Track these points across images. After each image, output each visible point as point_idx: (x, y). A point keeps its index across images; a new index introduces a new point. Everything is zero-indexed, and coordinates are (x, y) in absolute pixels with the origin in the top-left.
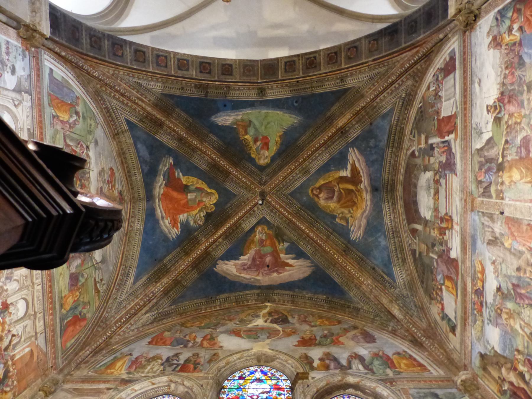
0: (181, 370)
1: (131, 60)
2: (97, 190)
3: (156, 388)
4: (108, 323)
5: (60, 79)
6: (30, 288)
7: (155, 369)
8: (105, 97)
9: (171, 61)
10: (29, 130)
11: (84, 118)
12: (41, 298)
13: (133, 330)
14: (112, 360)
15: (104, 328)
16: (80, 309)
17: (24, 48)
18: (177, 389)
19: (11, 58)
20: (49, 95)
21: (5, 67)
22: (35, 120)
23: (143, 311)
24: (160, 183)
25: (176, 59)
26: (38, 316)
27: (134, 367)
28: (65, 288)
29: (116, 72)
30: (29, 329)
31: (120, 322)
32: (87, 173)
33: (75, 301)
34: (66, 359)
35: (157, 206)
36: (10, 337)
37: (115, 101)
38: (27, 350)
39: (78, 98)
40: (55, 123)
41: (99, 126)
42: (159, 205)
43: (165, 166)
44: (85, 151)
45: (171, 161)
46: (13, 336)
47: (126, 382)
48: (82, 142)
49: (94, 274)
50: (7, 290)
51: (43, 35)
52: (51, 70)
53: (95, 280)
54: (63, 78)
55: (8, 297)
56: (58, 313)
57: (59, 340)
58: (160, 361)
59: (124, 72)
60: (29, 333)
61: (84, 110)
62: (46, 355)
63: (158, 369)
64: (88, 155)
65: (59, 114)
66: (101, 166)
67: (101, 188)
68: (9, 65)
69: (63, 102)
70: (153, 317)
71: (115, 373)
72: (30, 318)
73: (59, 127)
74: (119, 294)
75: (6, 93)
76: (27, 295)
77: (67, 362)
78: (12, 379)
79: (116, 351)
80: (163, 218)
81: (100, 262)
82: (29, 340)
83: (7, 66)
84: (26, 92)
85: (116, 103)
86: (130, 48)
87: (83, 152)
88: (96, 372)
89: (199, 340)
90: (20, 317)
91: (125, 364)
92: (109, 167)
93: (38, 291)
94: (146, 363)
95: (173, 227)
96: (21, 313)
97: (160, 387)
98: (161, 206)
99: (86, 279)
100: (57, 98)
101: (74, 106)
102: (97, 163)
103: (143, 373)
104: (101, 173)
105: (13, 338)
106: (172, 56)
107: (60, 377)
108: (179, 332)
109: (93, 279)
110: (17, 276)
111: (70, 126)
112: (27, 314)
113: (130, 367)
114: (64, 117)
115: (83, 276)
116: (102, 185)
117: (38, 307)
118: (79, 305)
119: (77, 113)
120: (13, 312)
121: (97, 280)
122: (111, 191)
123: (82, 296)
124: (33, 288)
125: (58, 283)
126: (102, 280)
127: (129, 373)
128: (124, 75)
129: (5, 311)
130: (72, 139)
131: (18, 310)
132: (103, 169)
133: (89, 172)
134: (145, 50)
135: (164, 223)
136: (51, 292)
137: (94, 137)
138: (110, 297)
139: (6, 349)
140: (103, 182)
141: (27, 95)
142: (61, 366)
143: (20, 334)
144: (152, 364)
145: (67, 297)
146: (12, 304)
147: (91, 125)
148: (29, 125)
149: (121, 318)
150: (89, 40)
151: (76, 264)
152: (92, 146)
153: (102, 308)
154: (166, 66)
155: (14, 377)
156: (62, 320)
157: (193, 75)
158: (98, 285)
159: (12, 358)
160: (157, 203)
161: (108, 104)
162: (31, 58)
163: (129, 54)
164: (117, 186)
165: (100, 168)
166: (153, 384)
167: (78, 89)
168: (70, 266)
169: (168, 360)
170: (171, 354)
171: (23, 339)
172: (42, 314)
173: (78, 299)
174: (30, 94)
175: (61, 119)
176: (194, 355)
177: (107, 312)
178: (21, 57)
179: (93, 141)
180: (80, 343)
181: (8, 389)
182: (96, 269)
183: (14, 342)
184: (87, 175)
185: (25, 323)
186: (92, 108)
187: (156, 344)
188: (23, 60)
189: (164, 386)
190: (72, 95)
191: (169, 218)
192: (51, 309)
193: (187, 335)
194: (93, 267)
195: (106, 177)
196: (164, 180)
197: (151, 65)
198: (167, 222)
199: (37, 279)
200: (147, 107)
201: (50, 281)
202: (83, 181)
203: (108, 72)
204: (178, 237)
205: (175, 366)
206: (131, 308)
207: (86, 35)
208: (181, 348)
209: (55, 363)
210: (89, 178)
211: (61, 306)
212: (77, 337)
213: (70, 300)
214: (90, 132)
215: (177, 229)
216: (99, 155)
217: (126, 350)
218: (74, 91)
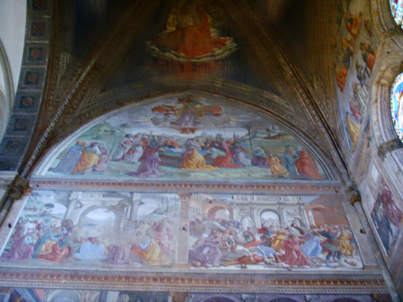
0: (371, 68)
1: (36, 88)
2: (173, 128)
3: (381, 98)
4: (314, 128)
5: (59, 161)
6: (253, 206)
7: (364, 95)
8: (77, 114)
9: (35, 44)
10: (104, 196)
11: (98, 138)
12: (265, 197)
13: (327, 104)
14: (347, 133)
15: (318, 133)
16: (290, 157)
17: (30, 194)
18: (388, 78)
19: (39, 207)
20: (73, 173)
21: (47, 213)
22: (95, 189)
23: (310, 89)
24: (173, 56)
25: (33, 38)
26: (282, 201)
27: (358, 115)
28: (264, 171)
29: (51, 103)
30: (291, 211)
31: (315, 116)
32: (154, 139)
33: (281, 163)
34: (334, 176)
35: (199, 61)
36: (293, 229)
37: (82, 104)
38: (310, 213)
39: (78, 143)
40: (100, 170)
41: (107, 121)
42: (198, 59)
43: (154, 49)
44: (131, 139)
45: (148, 43)
46: (292, 225)
47: (367, 127)
48: (122, 143)
49: (259, 139)
50: (249, 228)
51: (17, 178)
52: (50, 169)
53: (266, 138)
54: (57, 158)
55: (255, 227)
56: (286, 181)
57: (313, 182)
58: (359, 87)
59: (51, 95)
60: (295, 210)
61: (90, 137)
62: (322, 196)
63: (365, 92)
64: (136, 136)
65: (92, 165)
66: (148, 121)
67: (172, 123)
68: (45, 209)
69: (80, 160)
70: (319, 79)
71: (358, 134)
72: (282, 209)
73: (104, 166)
74: (287, 112)
75: (69, 214)
76: (259, 210)
77: (337, 176)
78: (332, 229)
79: (342, 126)
80: (213, 56)
81: (249, 130)
82: (301, 212)
83: (45, 211)
84: (70, 196)
85: (83, 102)
86: (24, 88)
87: (132, 142)
88: (353, 151)
89: (349, 37)
90: (278, 218)
91: (354, 122)
92: (151, 112)
93: (258, 199)
94: (357, 101)
95: (224, 44)
96: (274, 216)
97: (381, 95)
98: (199, 57)
99: (262, 148)
100: (77, 165)
101: (86, 148)
102: (146, 127)
103: (364, 108)
104: (156, 122)
105: (295, 225)
106: (29, 42)
107: (349, 184)
108: (338, 56)
109: (264, 140)
110: (238, 218)
111: (105, 154)
112: (277, 211)
113: (357, 119)
114: (95, 158)
115: (257, 152)
116: (168, 123)
117: (274, 200)
118: (286, 158)
119: (92, 145)
120: (270, 224)
121: (266, 136)
122: (177, 112)
123: (278, 154)
124: (254, 204)
125: (257, 179)
126: (268, 130)
127: (361, 121)
128: (53, 95)
129: (268, 231)
130: (117, 153)
131: (270, 219)
132: (152, 119)
133: (153, 136)
134: (25, 72)
135: (218, 54)
136: (263, 187)
137: (117, 128)
138: (288, 122)
139: (302, 232)
140: (166, 120)
141: (72, 195)
142: (339, 181)
143: (293, 219)
144: (359, 96)
145: (273, 170)
146: (262, 225)
147: (106, 131)
148: (100, 195)
149: (312, 114)
150: (19, 132)
151: (244, 158)
152: (127, 131)
153: (297, 133)
154: (41, 49)
155: (330, 227)
156: (293, 177)
157: (48, 19)
158: (272, 135)
159: (312, 227)
160: (196, 60)
161: (84, 111)
162: (39, 188)
163: (32, 90)
164: (173, 104)
165: (151, 124)
166: (376, 101)
167: (69, 143)
168: (244, 165)
169: (360, 78)
170: (355, 73)
171: (299, 217)
172: (282, 198)
173: (279, 159)
174: (72, 192)
175: (96, 163)
176: (361, 49)
177: (303, 128)
178: (38, 198)
179: (121, 129)
180: (324, 160)
181: (339, 234)
182: (255, 136)
183: (299, 225)
184: (156, 138)
185: (284, 213)
186: (88, 129)
187: (344, 85)
188: (41, 196)
189: (382, 90)
190: (74, 150)
191: (214, 49)
192: (280, 188)
193: (342, 48)
194: (252, 140)
195: (161, 116)
196: (170, 52)
197: (40, 67)
198: (218, 51)
199: (246, 200)
200: (87, 71)
201: (252, 187)
202: (161, 144)
203: (51, 111)
204: (235, 41)
205: (366, 74)
206: (304, 102)
207: (15, 134)
208: (352, 59)
209: (334, 188)
210: (158, 136)
211: (281, 177)
212: (317, 163)
213: (278, 167)
214: (113, 132)
215: (226, 40)
216: (137, 124)
217: (343, 116)
218: (70, 147)
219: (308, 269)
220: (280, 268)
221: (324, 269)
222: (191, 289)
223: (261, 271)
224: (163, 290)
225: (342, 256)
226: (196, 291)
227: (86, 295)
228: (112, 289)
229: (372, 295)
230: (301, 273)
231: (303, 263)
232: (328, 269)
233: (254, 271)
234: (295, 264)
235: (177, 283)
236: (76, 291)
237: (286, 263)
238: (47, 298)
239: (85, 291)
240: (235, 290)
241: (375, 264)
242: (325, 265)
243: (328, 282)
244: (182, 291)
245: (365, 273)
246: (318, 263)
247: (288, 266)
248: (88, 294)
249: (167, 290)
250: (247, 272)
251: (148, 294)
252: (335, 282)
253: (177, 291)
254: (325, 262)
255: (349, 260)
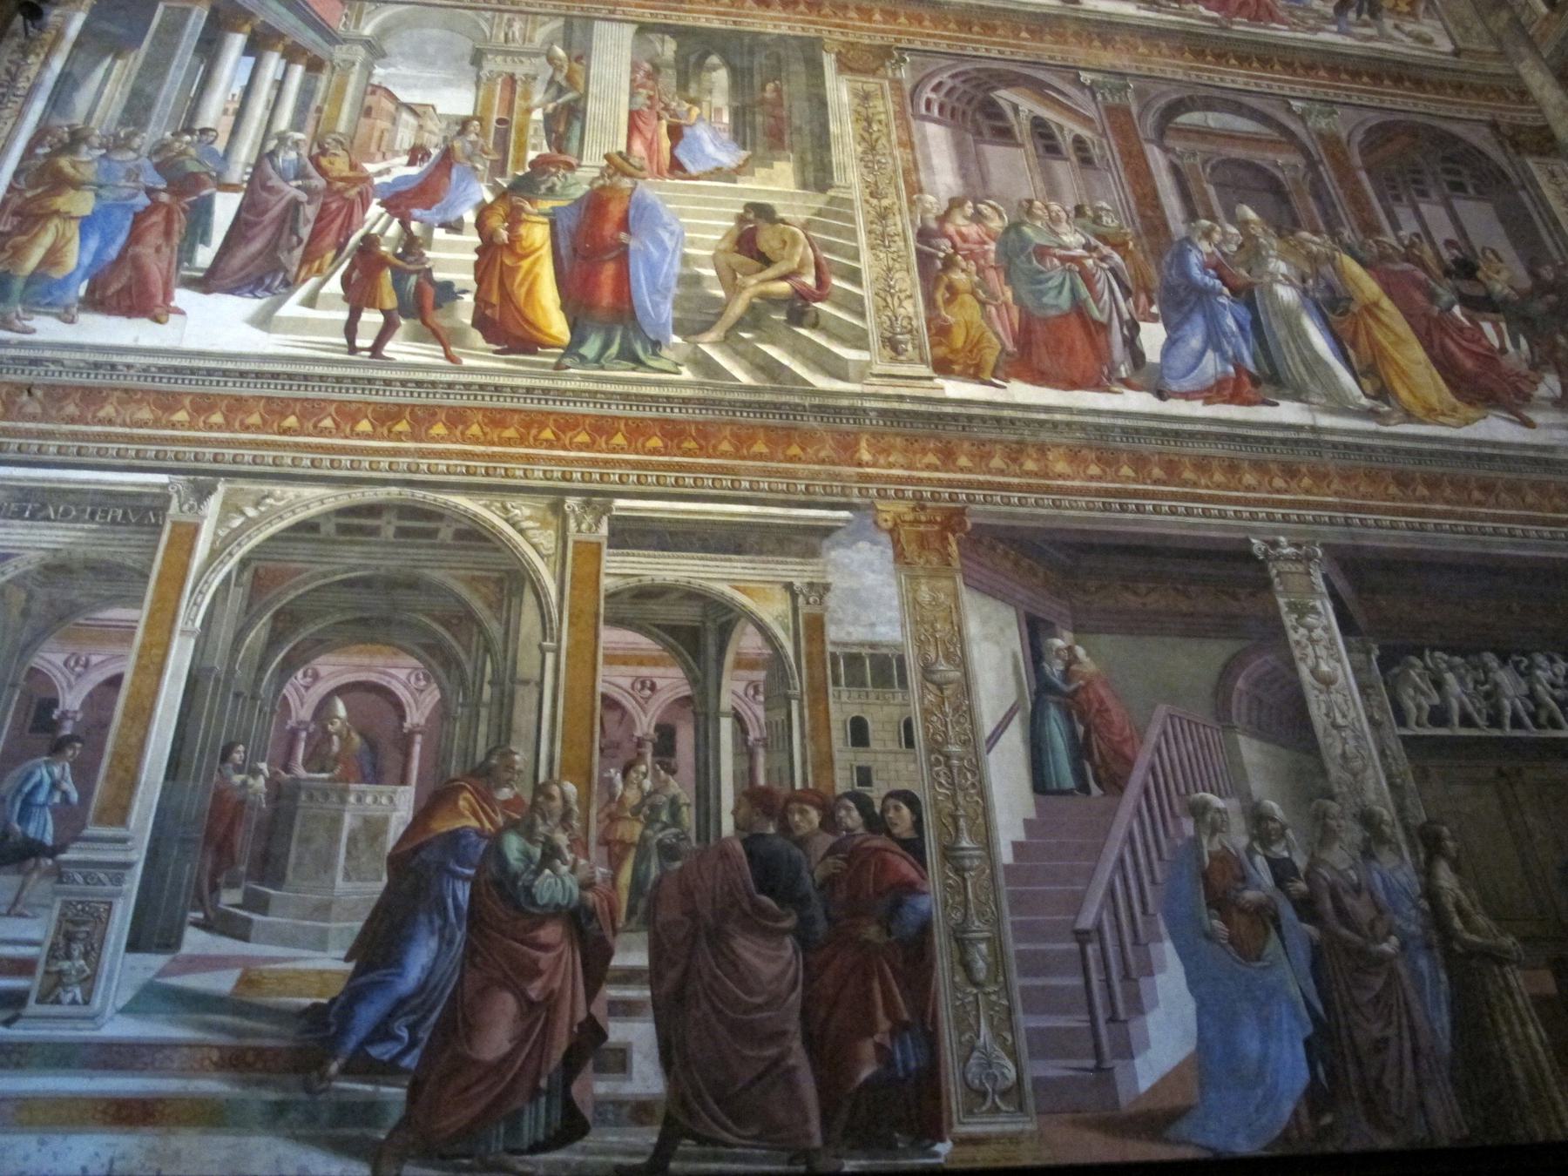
219: (1281, 32)
220: (1191, 16)
221: (1330, 37)
222: (899, 41)
223: (1131, 16)
224: (799, 33)
225: (1385, 12)
226: (917, 45)
227: (510, 25)
228: (603, 14)
229: (1494, 126)
230: (1261, 39)
231: (1262, 12)
232: (1349, 41)
233: (1109, 14)
234: (1237, 14)
235: (846, 18)
236: (469, 13)
237: (1207, 8)
238: (357, 26)
239: (506, 16)
240: (1051, 58)
241: (1492, 48)
242: (1335, 28)
243: (1355, 75)
244: (867, 41)
245: (1460, 66)
246: (1311, 22)
247: (1215, 14)
248: (517, 26)
249: (812, 33)
250: (1082, 15)
251: (747, 40)
252: (1376, 78)
253: (851, 39)
254: (1334, 22)
255: (1408, 27)
